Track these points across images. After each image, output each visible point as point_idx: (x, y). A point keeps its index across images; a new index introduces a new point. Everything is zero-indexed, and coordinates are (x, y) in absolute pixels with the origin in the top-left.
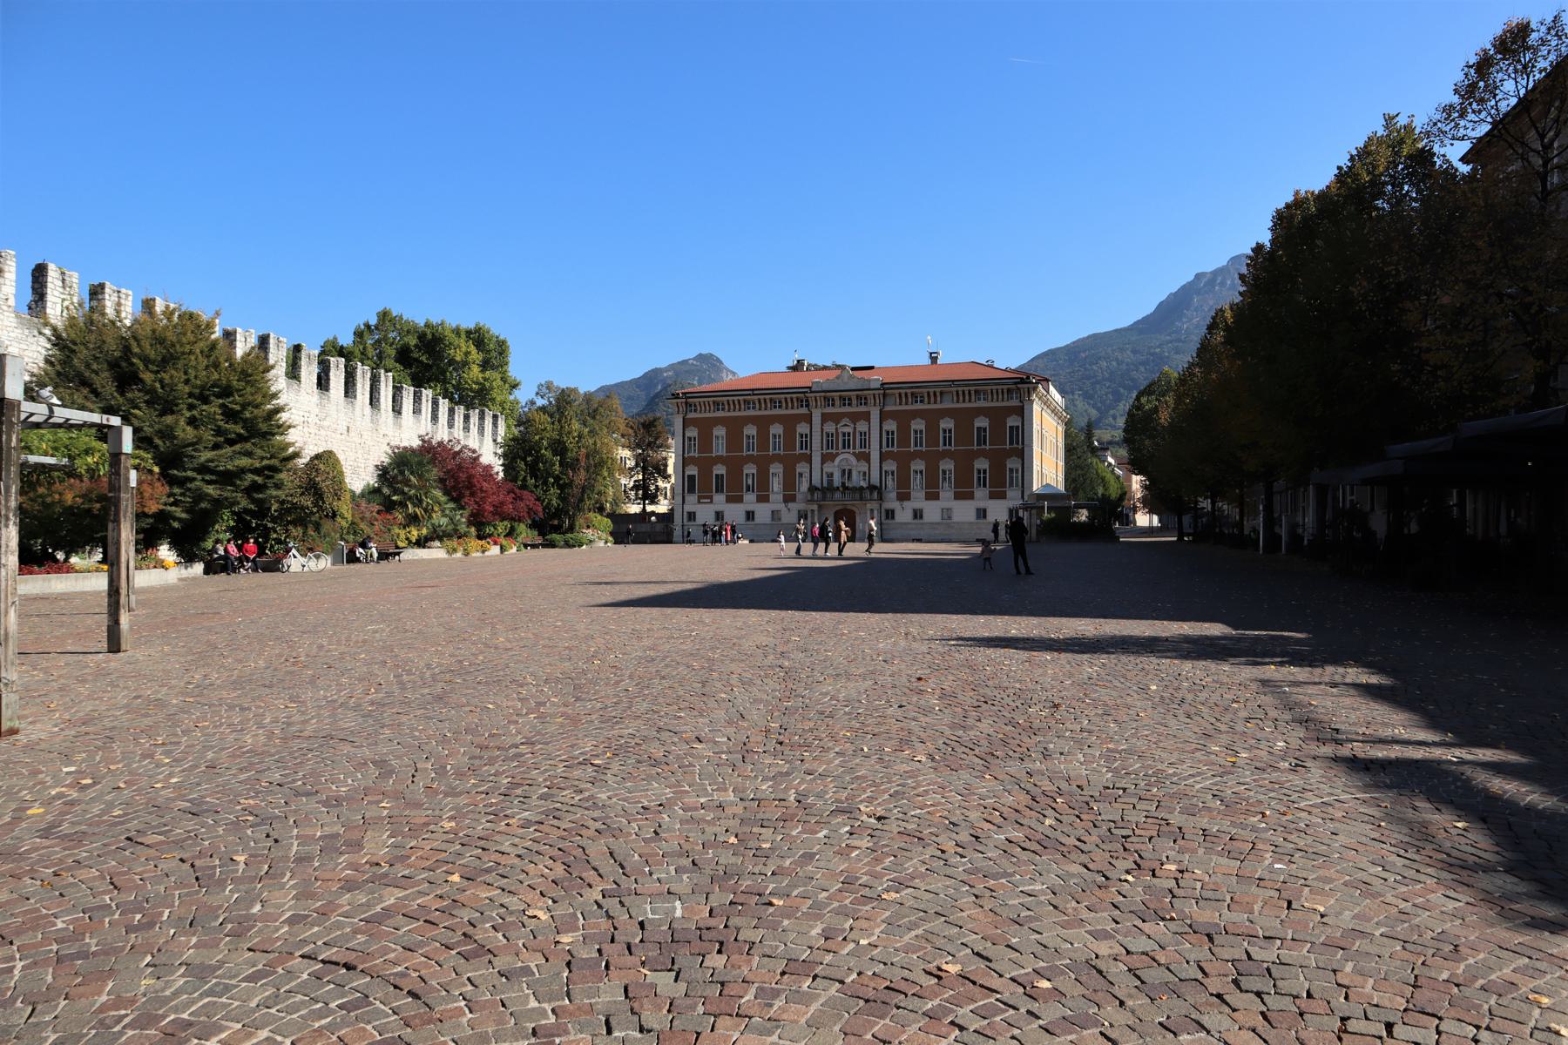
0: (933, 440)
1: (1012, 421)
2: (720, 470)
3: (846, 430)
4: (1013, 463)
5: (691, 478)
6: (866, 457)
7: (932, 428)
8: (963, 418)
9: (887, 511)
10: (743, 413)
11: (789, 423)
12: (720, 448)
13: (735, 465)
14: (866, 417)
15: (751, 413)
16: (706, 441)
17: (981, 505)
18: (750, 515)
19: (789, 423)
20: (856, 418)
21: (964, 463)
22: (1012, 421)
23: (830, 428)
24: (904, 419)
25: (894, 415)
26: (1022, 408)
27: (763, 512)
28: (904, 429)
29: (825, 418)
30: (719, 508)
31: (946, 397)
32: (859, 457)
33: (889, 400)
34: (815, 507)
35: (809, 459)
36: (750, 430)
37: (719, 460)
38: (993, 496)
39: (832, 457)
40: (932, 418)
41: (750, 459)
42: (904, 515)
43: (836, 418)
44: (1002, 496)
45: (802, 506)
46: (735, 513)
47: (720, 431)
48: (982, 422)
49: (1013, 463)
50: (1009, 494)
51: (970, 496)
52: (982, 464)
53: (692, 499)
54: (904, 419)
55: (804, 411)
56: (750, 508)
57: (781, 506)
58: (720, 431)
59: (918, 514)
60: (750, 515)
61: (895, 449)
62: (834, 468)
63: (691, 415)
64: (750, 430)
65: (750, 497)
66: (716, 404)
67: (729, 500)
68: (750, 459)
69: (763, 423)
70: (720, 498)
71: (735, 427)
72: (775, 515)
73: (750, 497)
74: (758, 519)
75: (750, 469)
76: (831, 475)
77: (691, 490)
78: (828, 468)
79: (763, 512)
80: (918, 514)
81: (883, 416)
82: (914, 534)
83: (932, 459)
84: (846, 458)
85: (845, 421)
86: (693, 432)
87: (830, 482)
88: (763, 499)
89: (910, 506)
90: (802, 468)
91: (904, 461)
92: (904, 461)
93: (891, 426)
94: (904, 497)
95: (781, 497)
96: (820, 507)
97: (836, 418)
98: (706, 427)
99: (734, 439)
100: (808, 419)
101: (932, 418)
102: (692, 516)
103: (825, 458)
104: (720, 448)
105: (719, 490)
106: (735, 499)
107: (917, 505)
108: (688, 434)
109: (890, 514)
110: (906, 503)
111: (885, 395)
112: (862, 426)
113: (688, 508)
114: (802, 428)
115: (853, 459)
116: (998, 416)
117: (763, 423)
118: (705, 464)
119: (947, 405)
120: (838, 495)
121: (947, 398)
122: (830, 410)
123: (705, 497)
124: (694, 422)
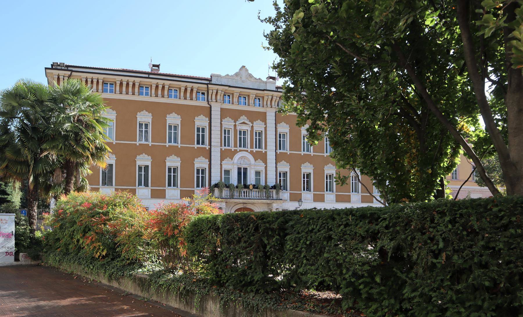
3: (244, 128)
6: (263, 157)
10: (136, 98)
14: (263, 117)
19: (188, 113)
20: (253, 116)
23: (229, 123)
29: (224, 113)
36: (144, 117)
41: (144, 149)
43: (235, 115)
64: (144, 117)
68: (144, 149)
69: (159, 111)
76: (227, 172)
84: (243, 158)
85: (243, 119)
92: (296, 162)
97: (235, 115)
103: (225, 155)
112: (259, 126)
122: (227, 106)
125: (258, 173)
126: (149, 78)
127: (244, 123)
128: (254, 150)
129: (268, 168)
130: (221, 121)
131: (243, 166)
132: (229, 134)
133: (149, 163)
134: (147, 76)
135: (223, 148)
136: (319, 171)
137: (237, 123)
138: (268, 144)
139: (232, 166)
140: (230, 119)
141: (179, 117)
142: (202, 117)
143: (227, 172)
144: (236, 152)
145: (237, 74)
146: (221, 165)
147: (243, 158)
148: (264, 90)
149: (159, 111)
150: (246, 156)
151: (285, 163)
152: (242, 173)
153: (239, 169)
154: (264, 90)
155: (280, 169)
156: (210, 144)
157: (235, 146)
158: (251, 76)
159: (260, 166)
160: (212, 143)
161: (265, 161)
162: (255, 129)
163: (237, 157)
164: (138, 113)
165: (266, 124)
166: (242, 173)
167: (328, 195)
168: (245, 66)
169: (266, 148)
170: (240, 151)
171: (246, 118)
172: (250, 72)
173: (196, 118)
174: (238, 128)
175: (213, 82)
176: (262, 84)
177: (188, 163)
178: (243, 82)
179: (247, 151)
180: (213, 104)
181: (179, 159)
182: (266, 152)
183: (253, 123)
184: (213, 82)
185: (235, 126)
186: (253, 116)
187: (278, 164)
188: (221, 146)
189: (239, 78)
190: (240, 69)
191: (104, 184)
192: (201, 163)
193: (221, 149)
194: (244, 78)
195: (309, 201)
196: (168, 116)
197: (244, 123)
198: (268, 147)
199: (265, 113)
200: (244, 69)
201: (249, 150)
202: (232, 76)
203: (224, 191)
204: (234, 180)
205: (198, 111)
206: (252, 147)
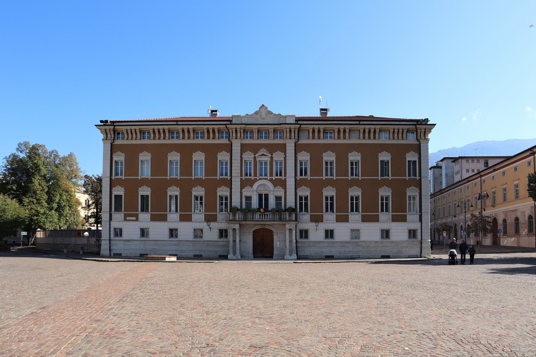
0: (342, 171)
1: (411, 157)
2: (145, 191)
4: (412, 192)
5: (118, 198)
6: (283, 184)
7: (342, 158)
8: (369, 152)
9: (301, 231)
11: (212, 152)
12: (146, 171)
13: (159, 186)
14: (283, 148)
15: (175, 141)
16: (132, 165)
17: (385, 226)
18: (173, 233)
19: (212, 152)
20: (272, 149)
21: (370, 189)
22: (411, 157)
23: (249, 156)
24: (316, 152)
25: (307, 148)
26: (419, 145)
27: (186, 230)
28: (316, 160)
29: (244, 148)
30: (144, 225)
31: (352, 135)
32: (276, 183)
33: (303, 135)
34: (237, 226)
35: (229, 184)
37: (145, 182)
38: (395, 219)
39: (251, 183)
40: (343, 152)
42: (316, 233)
43: (255, 148)
44: (403, 219)
45: (223, 226)
46: (159, 230)
47: (145, 157)
48: (385, 156)
49: (412, 192)
50: (409, 217)
51: (376, 219)
52: (385, 192)
53: (118, 216)
54: (316, 152)
55: (225, 141)
56: (173, 226)
57: (204, 225)
58: (145, 157)
59: (329, 234)
60: (173, 233)
61: (309, 177)
62: (252, 192)
63: (117, 142)
65: (173, 217)
66: (142, 132)
67: (154, 218)
68: (174, 182)
70: (145, 217)
71: (159, 156)
72: (198, 233)
73: (173, 217)
74: (182, 235)
75: (174, 191)
76: (249, 198)
77: (118, 209)
78: (247, 192)
79: (186, 230)
80: (329, 234)
81: (298, 148)
82: (327, 251)
83: (342, 187)
85: (263, 151)
86: (120, 157)
87: (249, 204)
88: (186, 218)
89: (323, 226)
90: (222, 191)
91: (317, 187)
92: (317, 187)
93: (305, 157)
94: (317, 219)
95: (202, 217)
96: (241, 226)
97: (255, 148)
98: (132, 153)
99: (159, 164)
100: (229, 148)
101: (343, 152)
102: (119, 232)
103: (244, 184)
104: (146, 171)
105: (144, 209)
106: (160, 217)
107: (330, 227)
108: (115, 158)
109: (304, 234)
110: (320, 224)
111: (299, 129)
112: (278, 156)
113: (114, 225)
114: (223, 156)
115: (270, 185)
116: (399, 151)
117: (186, 152)
118: (132, 186)
119: (354, 141)
120: (257, 216)
121: (355, 135)
123: (131, 214)
124: (122, 148)
125: (278, 199)
126: (177, 125)
127: (263, 155)
128: (274, 178)
129: (287, 193)
130: (241, 154)
131: (264, 192)
132: (250, 165)
133: (178, 193)
134: (175, 123)
135: (244, 178)
136: (342, 193)
137: (256, 156)
138: (287, 172)
139: (252, 192)
140: (250, 153)
141: (204, 154)
142: (224, 153)
143: (249, 198)
144: (255, 180)
145: (256, 113)
146: (241, 193)
147: (264, 185)
148: (280, 124)
149: (186, 152)
150: (265, 183)
151: (305, 188)
152: (263, 199)
153: (260, 196)
154: (280, 124)
155: (299, 193)
156: (231, 175)
157: (255, 175)
158: (270, 113)
159: (280, 192)
160: (233, 174)
161: (285, 188)
162: (274, 159)
163: (256, 185)
164: (169, 154)
165: (285, 154)
166: (263, 199)
167: (352, 216)
168: (263, 105)
169: (285, 175)
170: (260, 179)
171: (265, 150)
172: (269, 109)
173: (219, 154)
174: (258, 159)
175: (233, 122)
176: (282, 119)
177: (211, 192)
178: (263, 119)
179: (267, 179)
180: (233, 141)
181: (203, 189)
182: (285, 179)
183: (272, 154)
184: (233, 122)
185: (255, 157)
186: (272, 149)
187: (298, 189)
188: (241, 175)
189: (258, 116)
190: (260, 108)
191: (143, 210)
192: (222, 191)
193: (241, 179)
194: (263, 116)
195: (331, 222)
196: (194, 154)
197: (263, 155)
198: (287, 175)
199: (285, 145)
200: (263, 108)
201: (269, 178)
202: (252, 115)
203: (237, 215)
204: (255, 203)
205: (220, 148)
206: (271, 175)
